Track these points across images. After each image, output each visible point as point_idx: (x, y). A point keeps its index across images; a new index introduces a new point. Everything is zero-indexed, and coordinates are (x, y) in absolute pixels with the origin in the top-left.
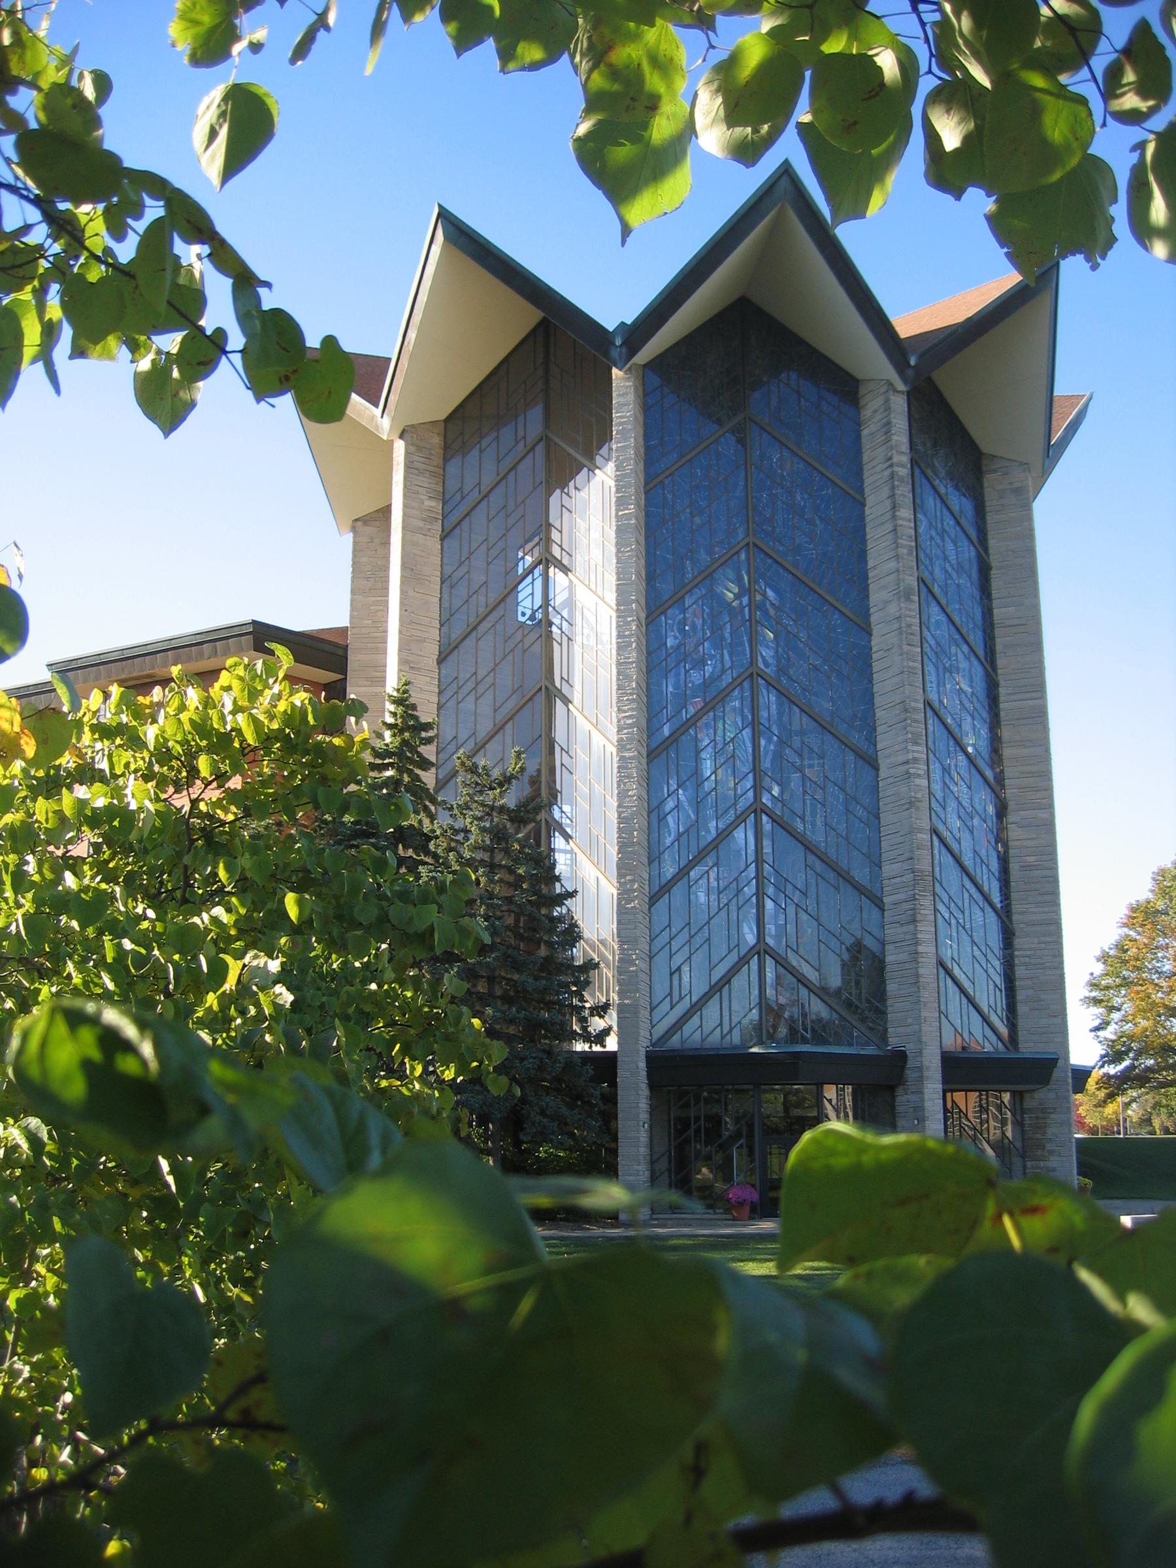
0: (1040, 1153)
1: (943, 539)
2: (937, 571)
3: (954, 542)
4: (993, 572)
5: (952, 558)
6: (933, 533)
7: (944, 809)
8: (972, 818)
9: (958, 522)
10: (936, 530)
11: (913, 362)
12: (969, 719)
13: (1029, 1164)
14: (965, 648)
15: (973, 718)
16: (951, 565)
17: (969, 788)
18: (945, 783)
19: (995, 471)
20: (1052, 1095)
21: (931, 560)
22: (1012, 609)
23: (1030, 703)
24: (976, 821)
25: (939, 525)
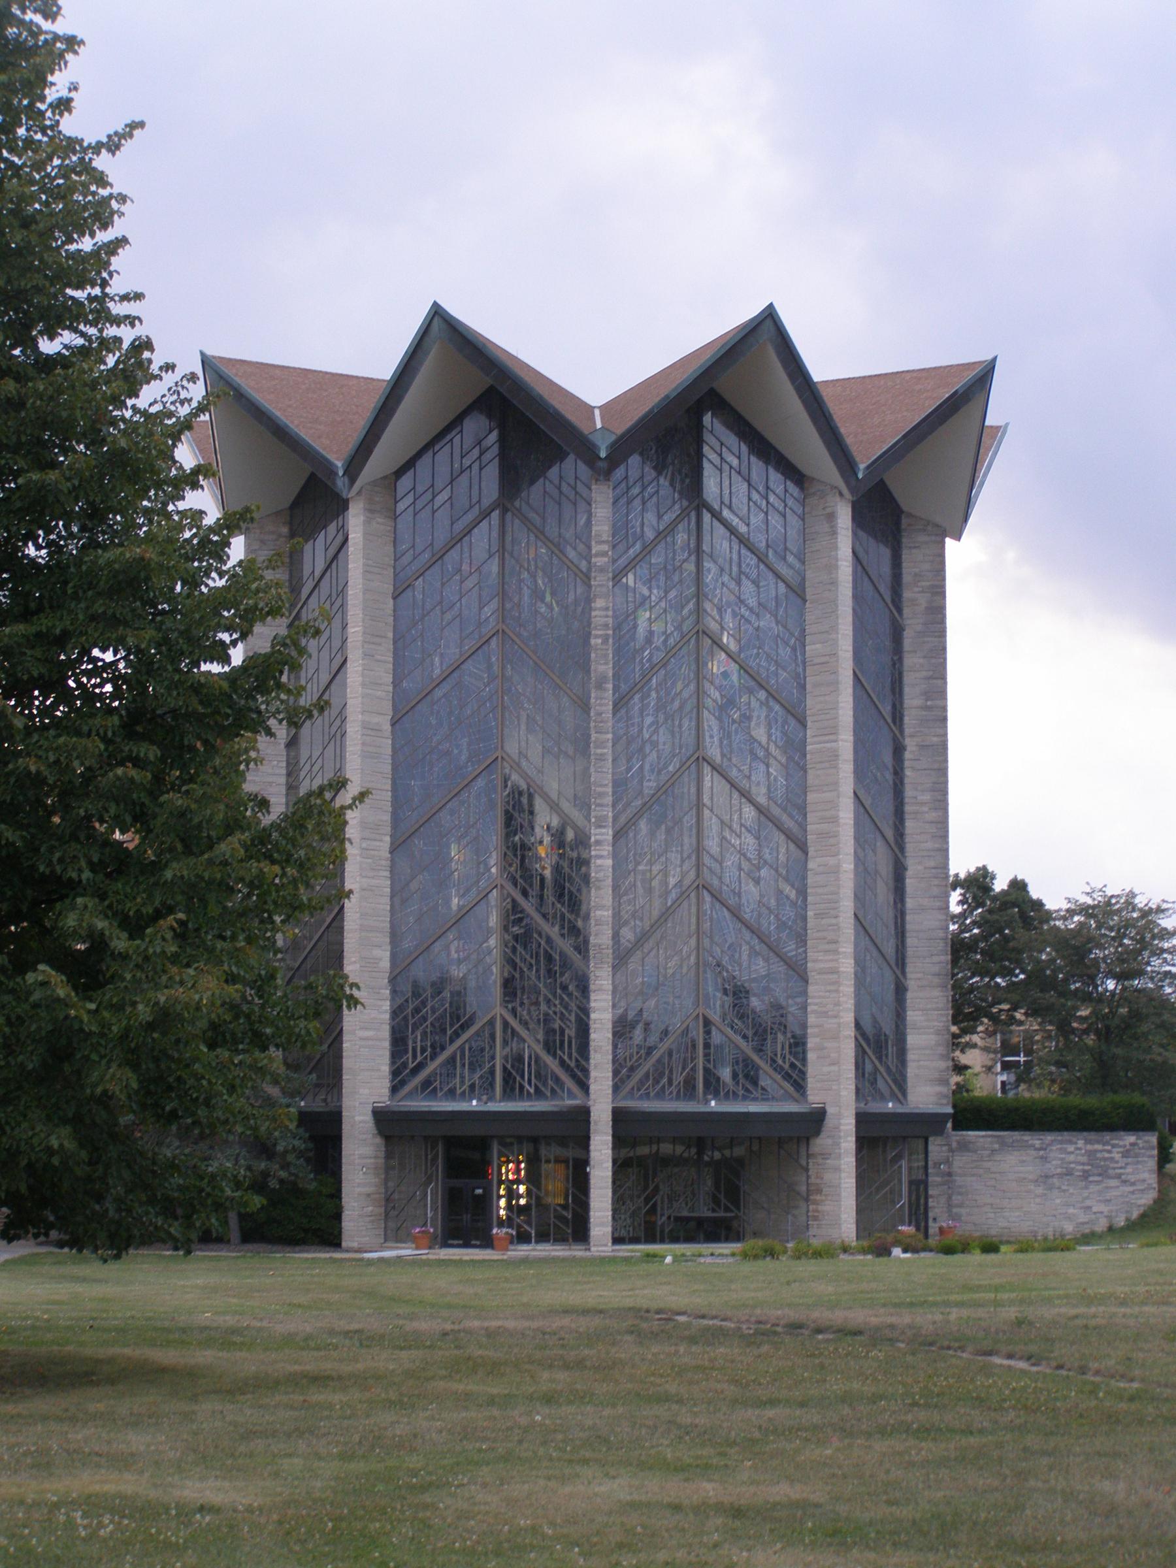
0: (818, 1197)
3: (756, 583)
4: (808, 605)
5: (752, 602)
6: (726, 578)
7: (721, 864)
8: (759, 869)
9: (762, 559)
10: (730, 575)
11: (603, 454)
12: (762, 767)
13: (811, 1207)
14: (762, 695)
15: (768, 766)
16: (751, 610)
17: (758, 838)
18: (723, 838)
19: (814, 494)
20: (829, 1141)
22: (818, 646)
23: (828, 745)
24: (764, 872)
25: (735, 569)
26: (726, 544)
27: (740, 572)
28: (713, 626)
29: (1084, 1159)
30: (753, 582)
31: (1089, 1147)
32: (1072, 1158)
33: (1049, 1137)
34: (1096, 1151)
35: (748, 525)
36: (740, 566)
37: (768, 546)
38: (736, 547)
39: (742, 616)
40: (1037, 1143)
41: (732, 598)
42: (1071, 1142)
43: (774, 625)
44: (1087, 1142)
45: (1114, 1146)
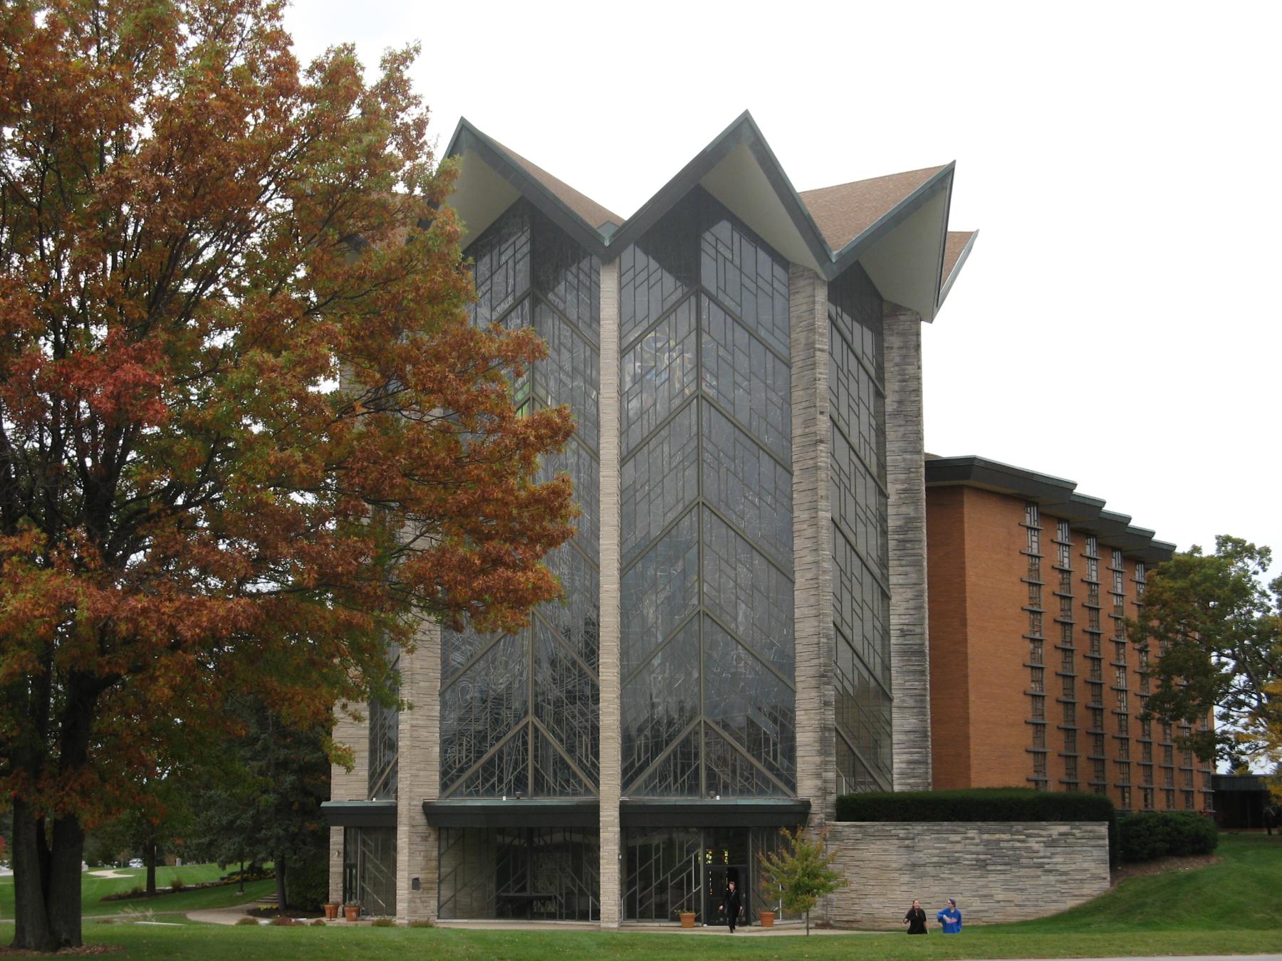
1: (559, 353)
2: (552, 383)
3: (571, 351)
5: (568, 367)
21: (546, 378)
26: (550, 322)
27: (560, 343)
28: (542, 392)
29: (980, 848)
30: (569, 350)
31: (986, 837)
32: (959, 847)
33: (918, 828)
34: (1000, 841)
35: (565, 302)
36: (559, 338)
37: (579, 318)
38: (557, 322)
39: (561, 381)
40: (902, 833)
41: (555, 367)
42: (955, 832)
43: (582, 384)
44: (981, 832)
45: (1028, 836)
